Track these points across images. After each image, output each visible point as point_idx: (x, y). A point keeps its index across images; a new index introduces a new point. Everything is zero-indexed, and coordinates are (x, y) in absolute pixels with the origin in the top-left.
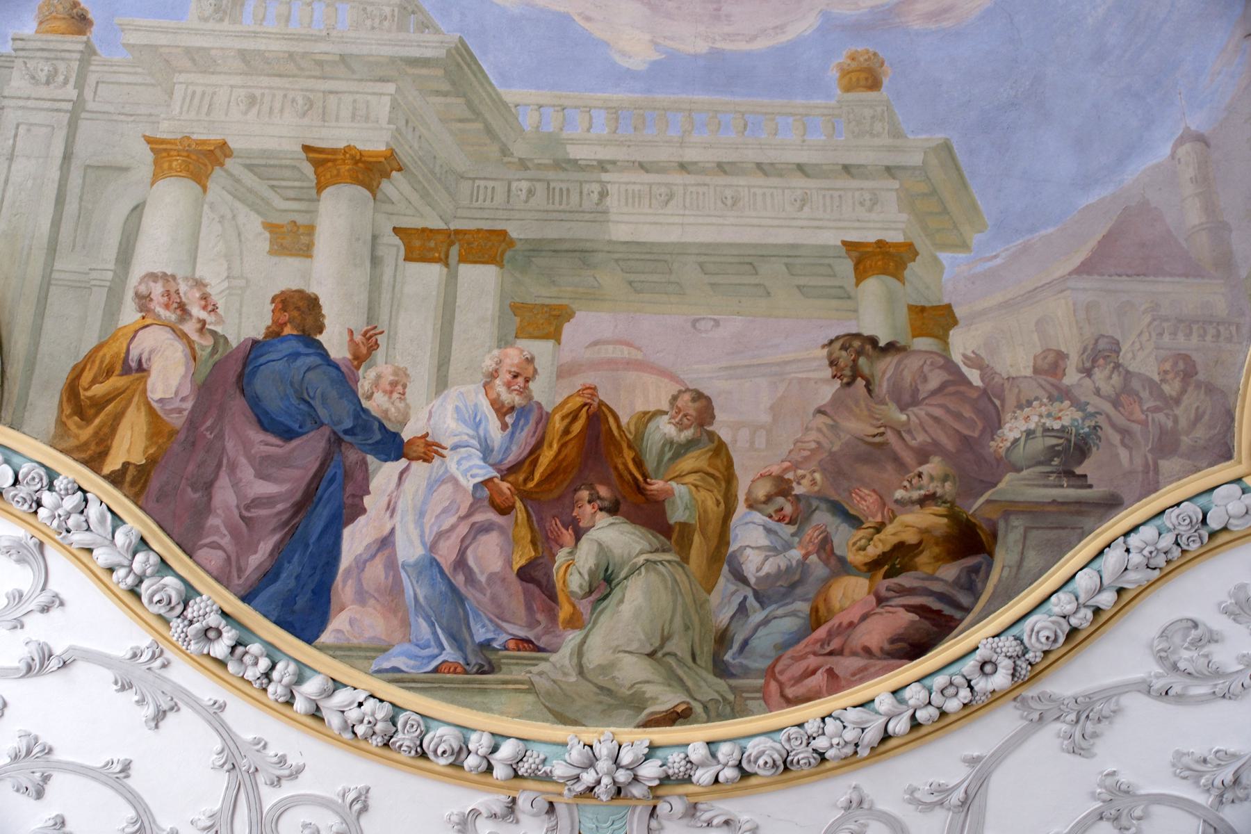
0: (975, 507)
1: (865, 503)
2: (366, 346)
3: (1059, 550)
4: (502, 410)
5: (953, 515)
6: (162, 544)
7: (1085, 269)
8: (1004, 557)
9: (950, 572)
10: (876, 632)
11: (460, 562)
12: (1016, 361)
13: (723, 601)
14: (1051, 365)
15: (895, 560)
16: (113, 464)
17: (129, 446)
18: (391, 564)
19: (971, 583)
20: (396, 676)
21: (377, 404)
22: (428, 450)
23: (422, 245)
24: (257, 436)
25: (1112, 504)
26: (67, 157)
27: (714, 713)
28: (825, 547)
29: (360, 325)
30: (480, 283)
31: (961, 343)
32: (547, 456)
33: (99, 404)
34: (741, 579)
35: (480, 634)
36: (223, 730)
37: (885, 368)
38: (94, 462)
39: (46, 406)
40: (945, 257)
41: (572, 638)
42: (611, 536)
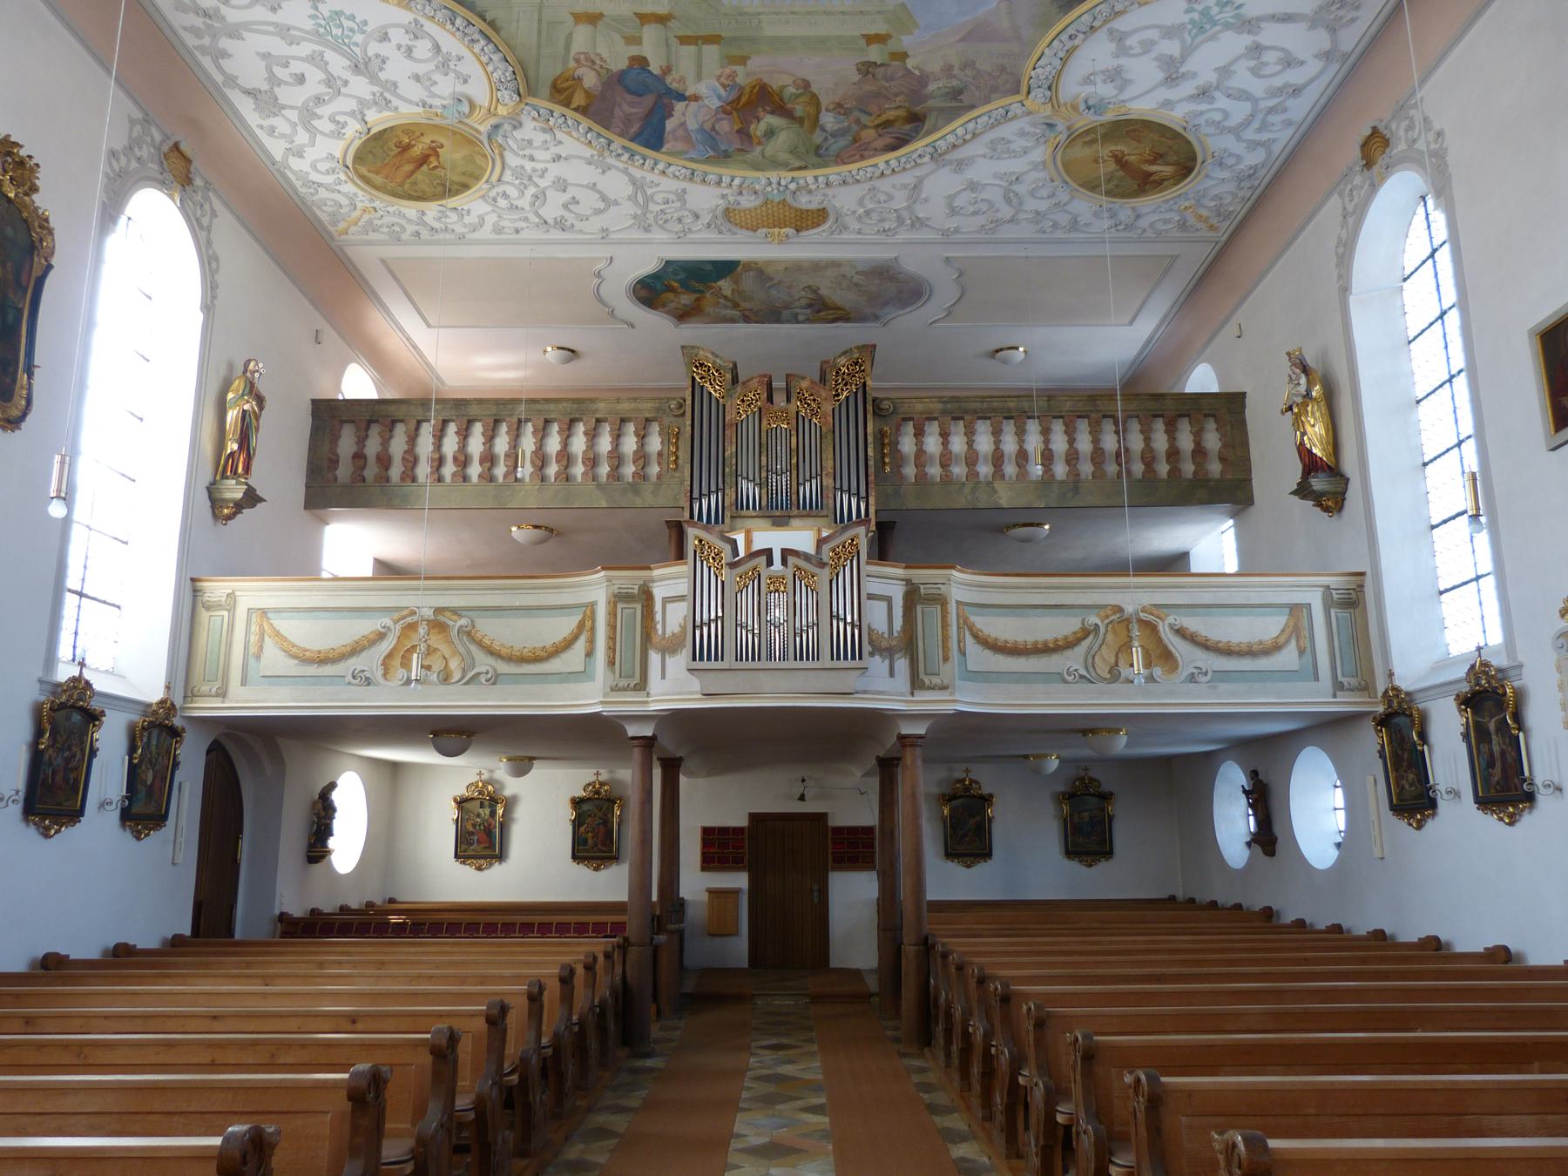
0: (918, 109)
1: (874, 108)
2: (667, 70)
3: (951, 120)
4: (724, 86)
5: (908, 111)
6: (597, 128)
7: (963, 40)
8: (928, 124)
9: (908, 127)
10: (879, 143)
11: (713, 128)
12: (934, 66)
13: (818, 137)
14: (948, 69)
15: (887, 124)
16: (574, 105)
17: (579, 99)
18: (686, 130)
19: (917, 131)
20: (692, 160)
21: (675, 86)
22: (696, 98)
23: (684, 40)
24: (629, 98)
25: (972, 107)
26: (540, 20)
27: (815, 167)
28: (858, 121)
29: (664, 64)
30: (712, 52)
31: (910, 63)
32: (744, 99)
33: (566, 89)
34: (823, 129)
35: (723, 148)
36: (629, 175)
37: (880, 72)
38: (567, 104)
39: (546, 91)
40: (904, 38)
41: (759, 149)
42: (770, 120)
